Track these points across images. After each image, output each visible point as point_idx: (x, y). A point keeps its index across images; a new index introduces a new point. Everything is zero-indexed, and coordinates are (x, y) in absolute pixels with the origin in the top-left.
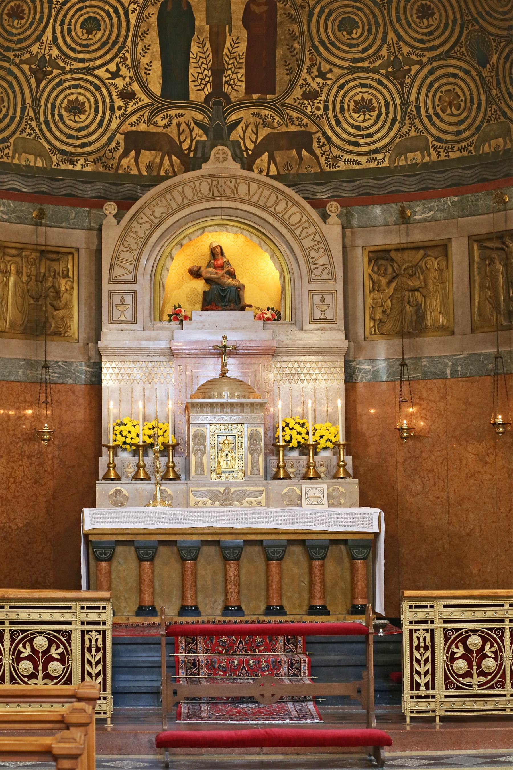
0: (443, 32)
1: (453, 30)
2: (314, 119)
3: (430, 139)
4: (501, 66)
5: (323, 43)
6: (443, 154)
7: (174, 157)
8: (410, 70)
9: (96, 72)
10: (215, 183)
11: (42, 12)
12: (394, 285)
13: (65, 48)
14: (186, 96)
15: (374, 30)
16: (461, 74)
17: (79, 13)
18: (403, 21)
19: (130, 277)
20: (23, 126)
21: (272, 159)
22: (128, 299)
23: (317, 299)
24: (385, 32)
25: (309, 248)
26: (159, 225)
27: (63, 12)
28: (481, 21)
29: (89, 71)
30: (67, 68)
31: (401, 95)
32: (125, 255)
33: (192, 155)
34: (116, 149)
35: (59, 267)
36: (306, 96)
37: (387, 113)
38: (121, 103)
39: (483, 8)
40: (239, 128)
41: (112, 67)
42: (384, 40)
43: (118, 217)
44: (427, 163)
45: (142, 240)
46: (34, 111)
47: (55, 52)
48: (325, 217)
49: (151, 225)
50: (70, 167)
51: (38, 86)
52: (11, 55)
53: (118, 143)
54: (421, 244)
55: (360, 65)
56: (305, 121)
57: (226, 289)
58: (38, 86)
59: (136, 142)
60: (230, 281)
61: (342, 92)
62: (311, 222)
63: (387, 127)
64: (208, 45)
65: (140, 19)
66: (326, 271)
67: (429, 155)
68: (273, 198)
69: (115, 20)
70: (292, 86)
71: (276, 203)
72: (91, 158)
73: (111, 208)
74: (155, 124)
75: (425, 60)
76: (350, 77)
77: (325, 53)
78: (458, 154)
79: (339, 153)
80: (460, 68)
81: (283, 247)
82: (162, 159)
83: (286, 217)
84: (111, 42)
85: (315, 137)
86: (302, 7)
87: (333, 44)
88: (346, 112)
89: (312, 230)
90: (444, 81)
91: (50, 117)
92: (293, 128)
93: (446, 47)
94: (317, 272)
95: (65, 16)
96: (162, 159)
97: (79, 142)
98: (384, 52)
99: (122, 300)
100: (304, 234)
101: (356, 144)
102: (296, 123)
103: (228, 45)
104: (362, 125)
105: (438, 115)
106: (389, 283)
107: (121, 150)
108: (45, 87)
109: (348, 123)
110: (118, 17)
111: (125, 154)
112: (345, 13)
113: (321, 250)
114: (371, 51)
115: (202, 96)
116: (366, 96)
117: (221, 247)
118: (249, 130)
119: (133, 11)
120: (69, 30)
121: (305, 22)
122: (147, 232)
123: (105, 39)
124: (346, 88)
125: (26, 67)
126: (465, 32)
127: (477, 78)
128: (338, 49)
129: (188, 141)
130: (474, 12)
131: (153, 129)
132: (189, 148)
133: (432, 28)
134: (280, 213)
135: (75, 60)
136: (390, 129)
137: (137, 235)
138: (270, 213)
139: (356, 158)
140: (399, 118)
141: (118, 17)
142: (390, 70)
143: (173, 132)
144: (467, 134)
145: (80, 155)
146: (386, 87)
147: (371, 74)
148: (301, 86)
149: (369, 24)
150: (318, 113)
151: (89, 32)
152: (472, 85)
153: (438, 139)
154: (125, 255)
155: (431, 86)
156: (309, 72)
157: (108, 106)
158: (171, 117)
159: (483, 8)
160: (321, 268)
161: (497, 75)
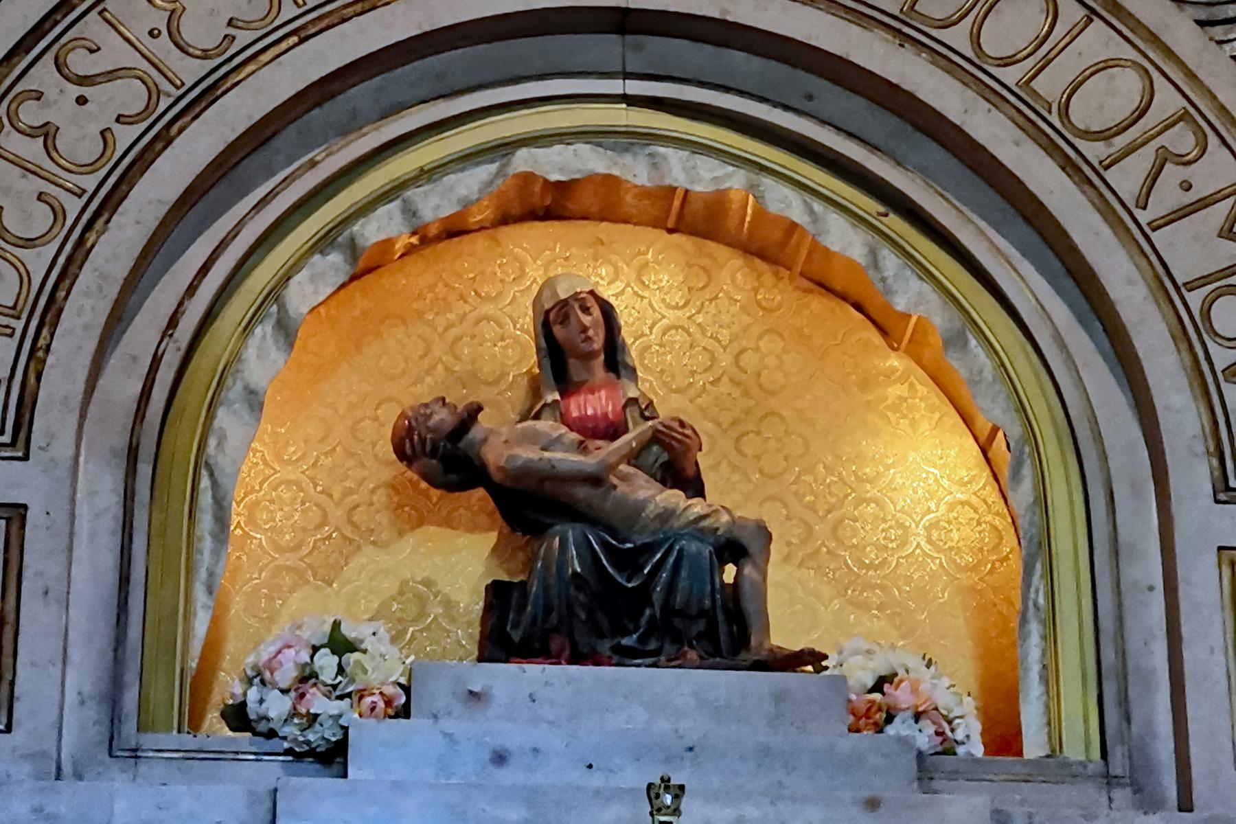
25: (1203, 281)
26: (208, 94)
45: (90, 183)
49: (154, 93)
57: (649, 549)
60: (673, 497)
81: (1029, 284)
100: (1167, 196)
117: (608, 311)
122: (125, 136)
134: (1007, 62)
137: (50, 148)
138: (943, 58)
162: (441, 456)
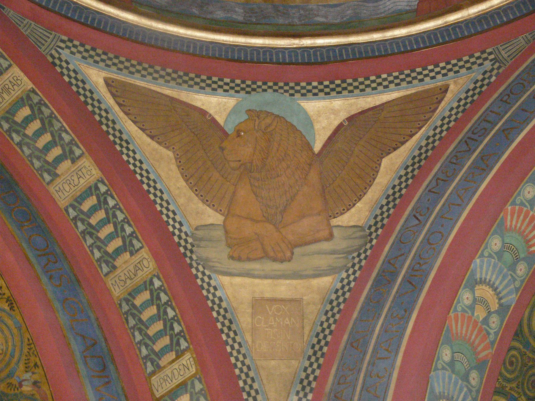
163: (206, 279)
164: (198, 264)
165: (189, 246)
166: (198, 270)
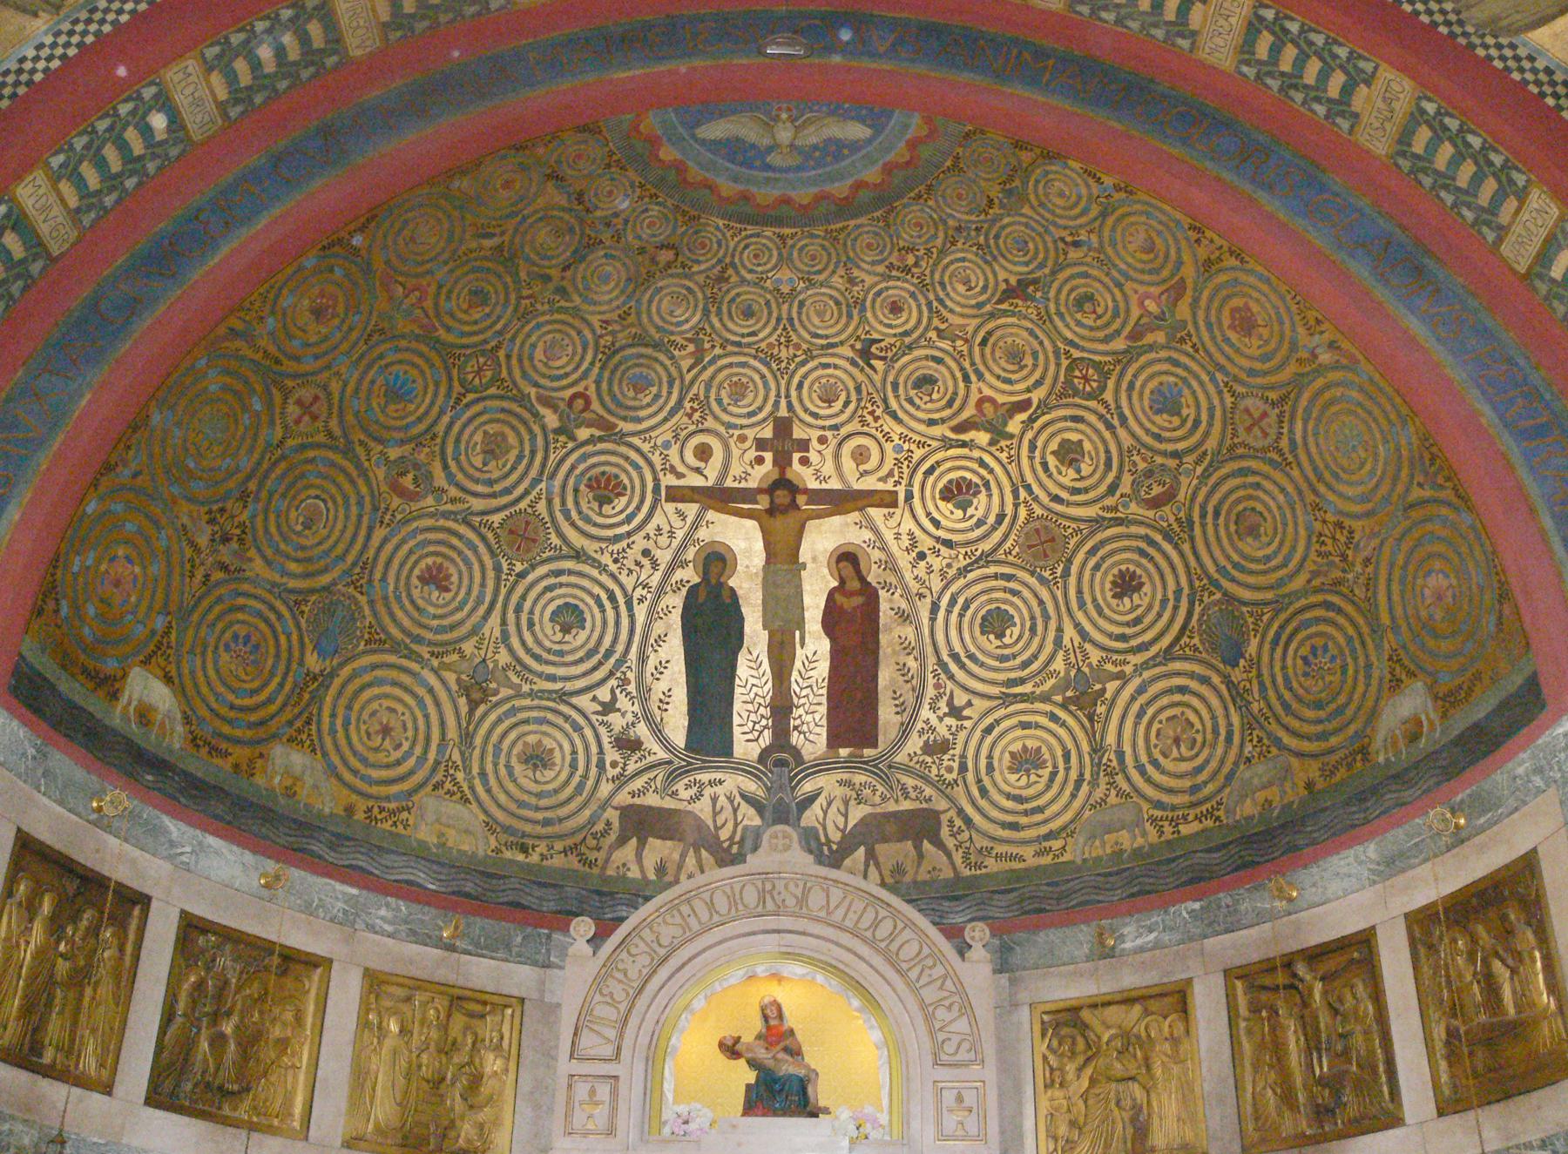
0: (1159, 615)
1: (1176, 608)
2: (943, 786)
3: (1145, 806)
4: (1265, 659)
5: (955, 657)
6: (1168, 829)
7: (704, 853)
8: (1104, 690)
9: (574, 700)
10: (768, 886)
11: (483, 585)
12: (1089, 1071)
13: (521, 653)
14: (726, 749)
15: (1040, 628)
16: (1194, 685)
17: (549, 595)
18: (1090, 606)
19: (608, 1051)
20: (439, 777)
21: (871, 855)
22: (604, 1091)
23: (949, 1097)
24: (1060, 630)
26: (665, 959)
27: (520, 590)
28: (1225, 584)
29: (563, 697)
30: (526, 688)
31: (1091, 736)
32: (603, 1011)
33: (735, 849)
34: (604, 834)
35: (487, 1029)
36: (928, 749)
37: (1067, 769)
38: (617, 757)
39: (1228, 558)
40: (816, 808)
41: (604, 694)
42: (1058, 642)
43: (596, 940)
44: (1141, 848)
46: (462, 754)
47: (504, 657)
48: (963, 949)
50: (521, 857)
51: (471, 712)
52: (424, 651)
53: (608, 823)
54: (1134, 994)
55: (1018, 690)
56: (928, 791)
58: (471, 712)
59: (642, 823)
61: (989, 740)
62: (938, 958)
63: (1067, 793)
64: (766, 666)
65: (652, 615)
66: (966, 1045)
67: (1144, 834)
68: (869, 916)
69: (610, 613)
70: (905, 731)
71: (875, 925)
72: (559, 846)
73: (583, 927)
74: (674, 794)
75: (1128, 669)
76: (1002, 712)
77: (960, 675)
78: (1195, 827)
79: (986, 843)
80: (1192, 675)
82: (683, 856)
83: (894, 947)
84: (602, 650)
85: (944, 818)
86: (921, 596)
87: (972, 657)
88: (997, 774)
89: (939, 971)
90: (1165, 701)
91: (489, 768)
92: (906, 805)
93: (1166, 641)
94: (949, 1048)
95: (524, 597)
96: (683, 856)
97: (540, 816)
98: (1058, 665)
99: (593, 1092)
101: (1014, 826)
102: (913, 795)
103: (798, 664)
104: (1024, 793)
105: (1155, 763)
106: (1080, 1069)
107: (613, 837)
108: (486, 714)
109: (1000, 791)
110: (616, 608)
111: (622, 841)
112: (990, 601)
113: (956, 1007)
114: (1035, 666)
115: (754, 751)
116: (1030, 744)
118: (833, 808)
119: (641, 601)
120: (531, 624)
121: (926, 621)
123: (591, 644)
124: (996, 732)
125: (451, 678)
126: (1198, 609)
127: (1223, 688)
128: (982, 665)
129: (730, 825)
130: (1211, 569)
131: (669, 803)
132: (731, 838)
133: (1139, 611)
135: (540, 675)
136: (1073, 796)
139: (1015, 850)
140: (1087, 776)
141: (616, 608)
142: (1069, 694)
143: (703, 808)
144: (1210, 788)
145: (539, 838)
146: (1064, 724)
147: (1039, 706)
148: (921, 732)
149: (1033, 618)
150: (950, 777)
151: (566, 629)
152: (1215, 702)
153: (1158, 805)
154: (603, 1011)
155: (1140, 715)
156: (933, 708)
157: (594, 760)
158: (701, 785)
159: (1228, 558)
160: (956, 1039)
161: (1259, 675)
162: (731, 1049)
163: (1508, 53)
164: (1483, 36)
165: (1452, 17)
166: (1486, 47)
